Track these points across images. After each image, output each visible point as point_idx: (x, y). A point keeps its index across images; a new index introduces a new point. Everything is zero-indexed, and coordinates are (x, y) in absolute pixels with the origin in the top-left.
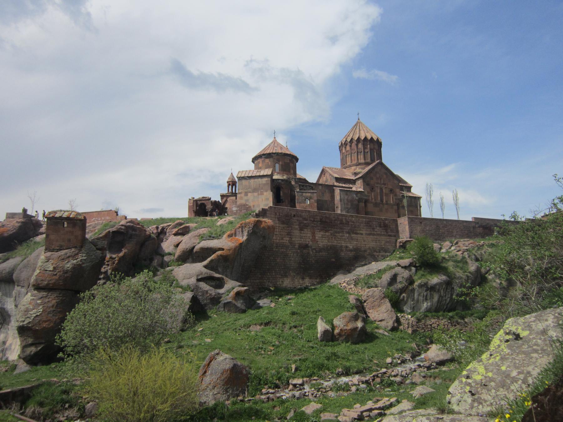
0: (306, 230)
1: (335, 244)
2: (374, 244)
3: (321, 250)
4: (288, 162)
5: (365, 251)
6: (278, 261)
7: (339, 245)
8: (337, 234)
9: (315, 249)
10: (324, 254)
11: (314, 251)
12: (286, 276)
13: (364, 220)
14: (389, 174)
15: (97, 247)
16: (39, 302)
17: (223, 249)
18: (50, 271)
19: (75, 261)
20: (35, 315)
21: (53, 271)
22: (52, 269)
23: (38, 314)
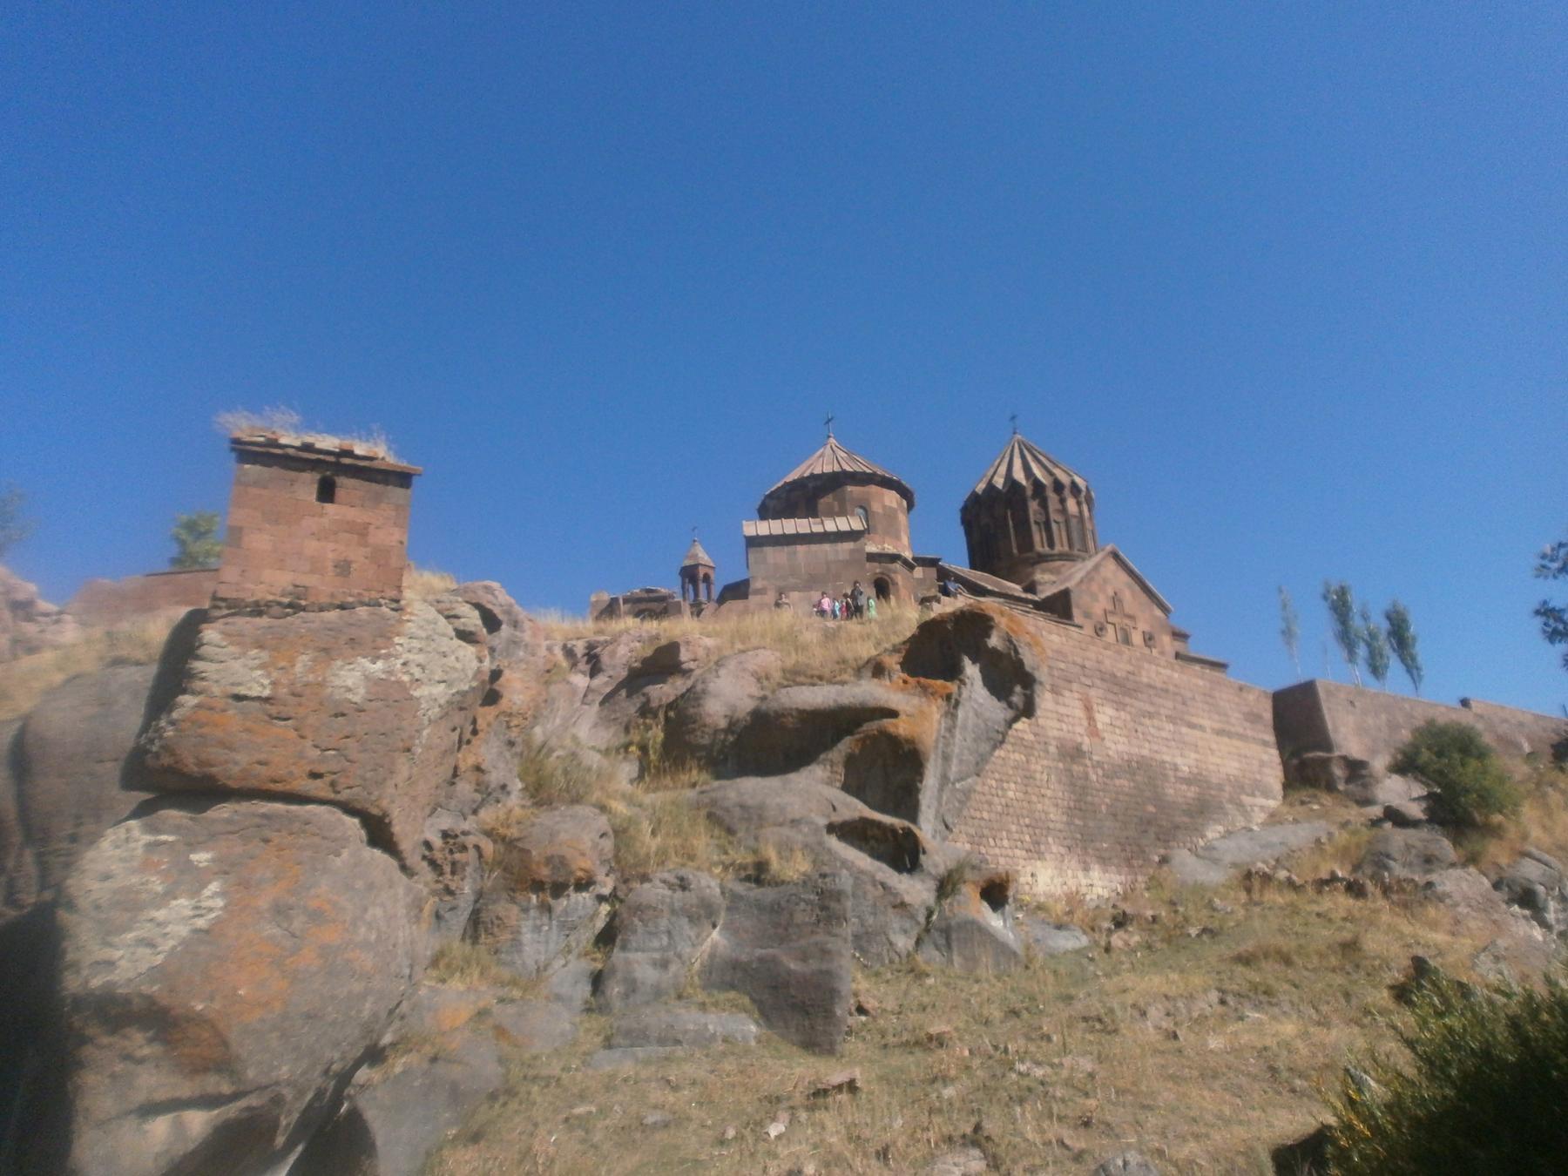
0: (1067, 693)
1: (1145, 752)
2: (1236, 764)
3: (1112, 772)
4: (894, 505)
5: (1220, 788)
6: (1011, 794)
7: (1158, 757)
8: (1147, 721)
9: (1099, 764)
10: (1123, 783)
11: (1100, 772)
12: (1040, 856)
13: (1201, 683)
14: (1137, 588)
15: (458, 623)
16: (201, 858)
17: (893, 714)
18: (259, 698)
19: (380, 664)
20: (183, 931)
21: (267, 700)
22: (266, 693)
23: (201, 923)
